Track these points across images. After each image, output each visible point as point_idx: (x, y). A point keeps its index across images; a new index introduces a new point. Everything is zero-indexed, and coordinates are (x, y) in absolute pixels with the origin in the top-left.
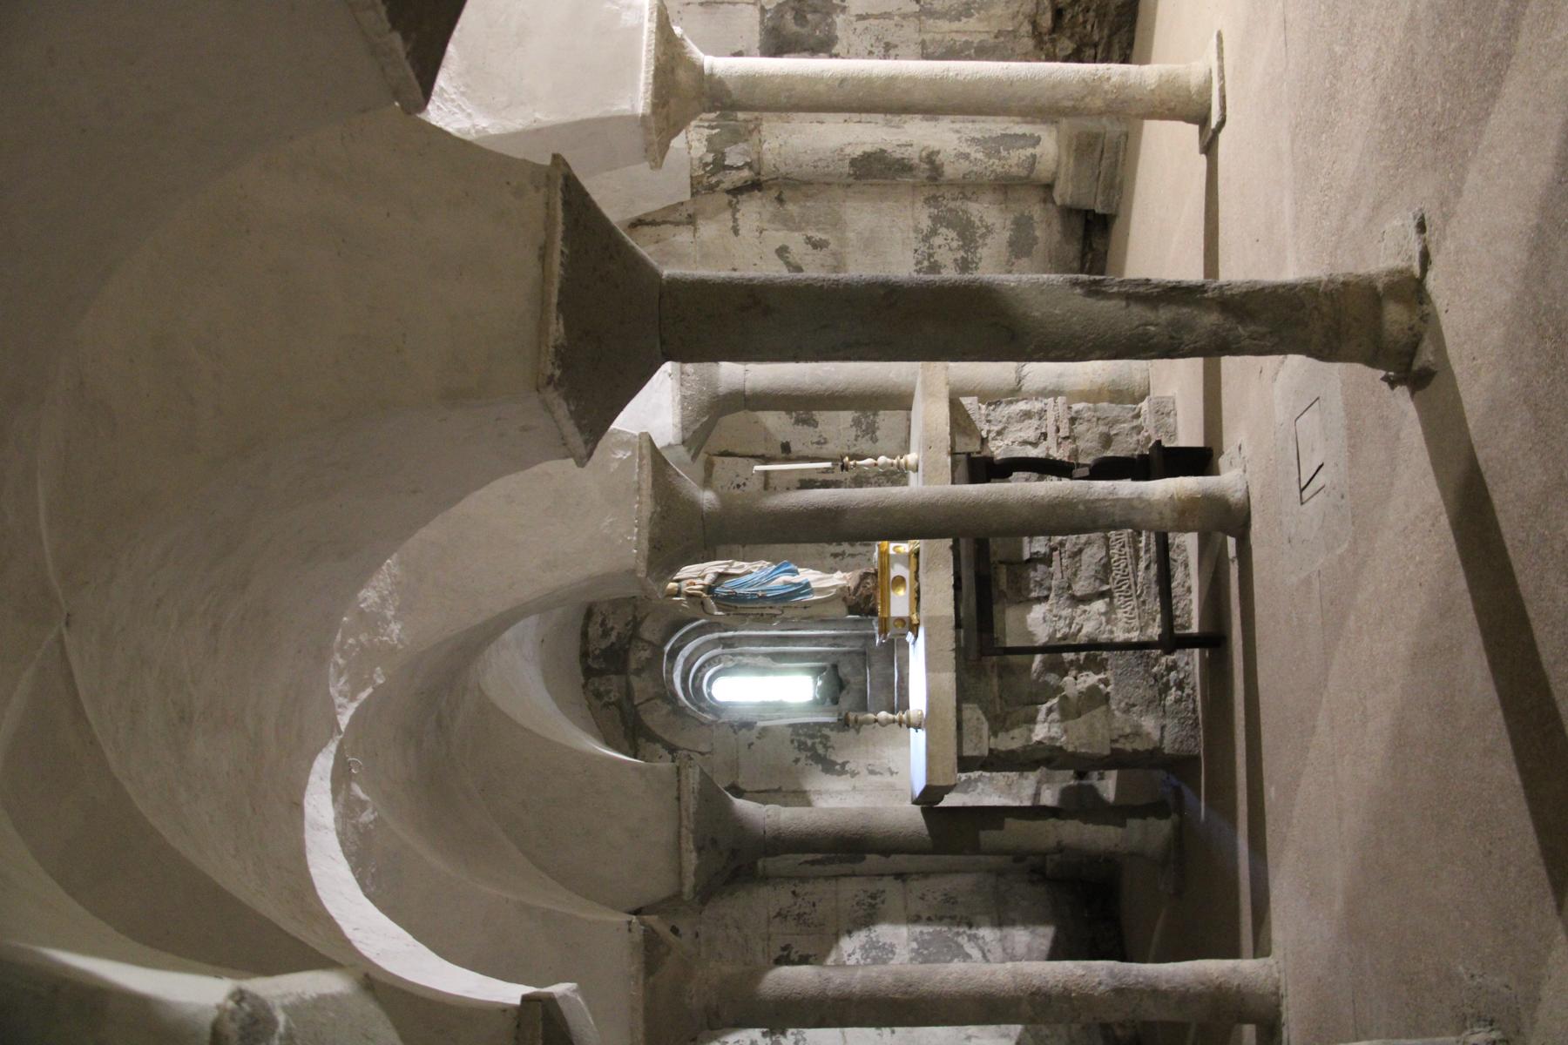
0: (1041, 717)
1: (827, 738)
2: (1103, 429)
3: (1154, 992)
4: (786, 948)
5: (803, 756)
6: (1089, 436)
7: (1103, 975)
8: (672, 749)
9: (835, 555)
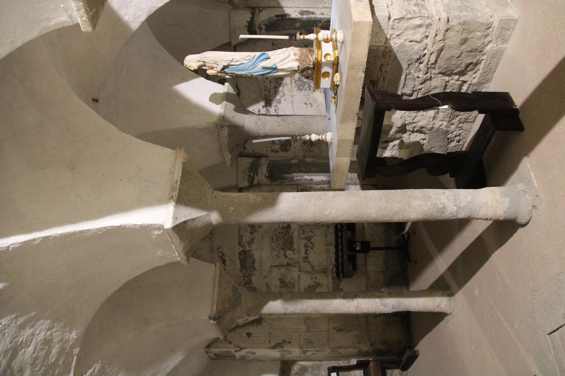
0: (389, 148)
2: (464, 36)
6: (454, 39)
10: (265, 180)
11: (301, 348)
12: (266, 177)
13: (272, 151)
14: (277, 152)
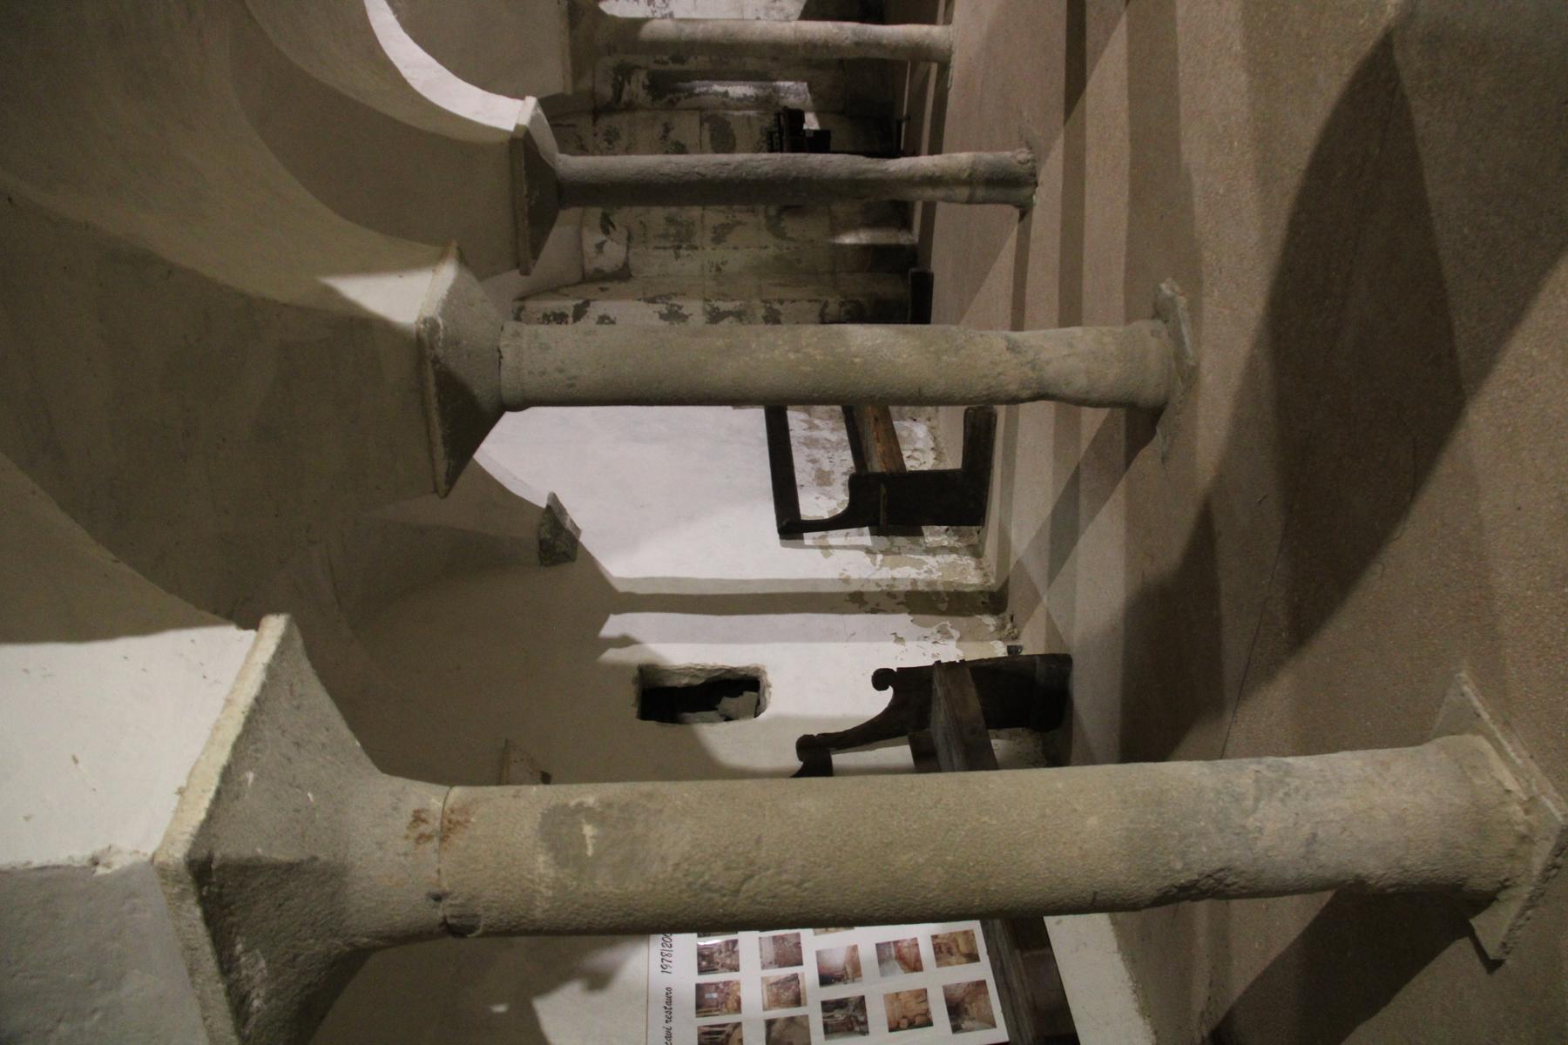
3: (878, 44)
7: (849, 33)
10: (643, 96)
11: (706, 300)
12: (644, 87)
13: (657, 62)
14: (665, 63)
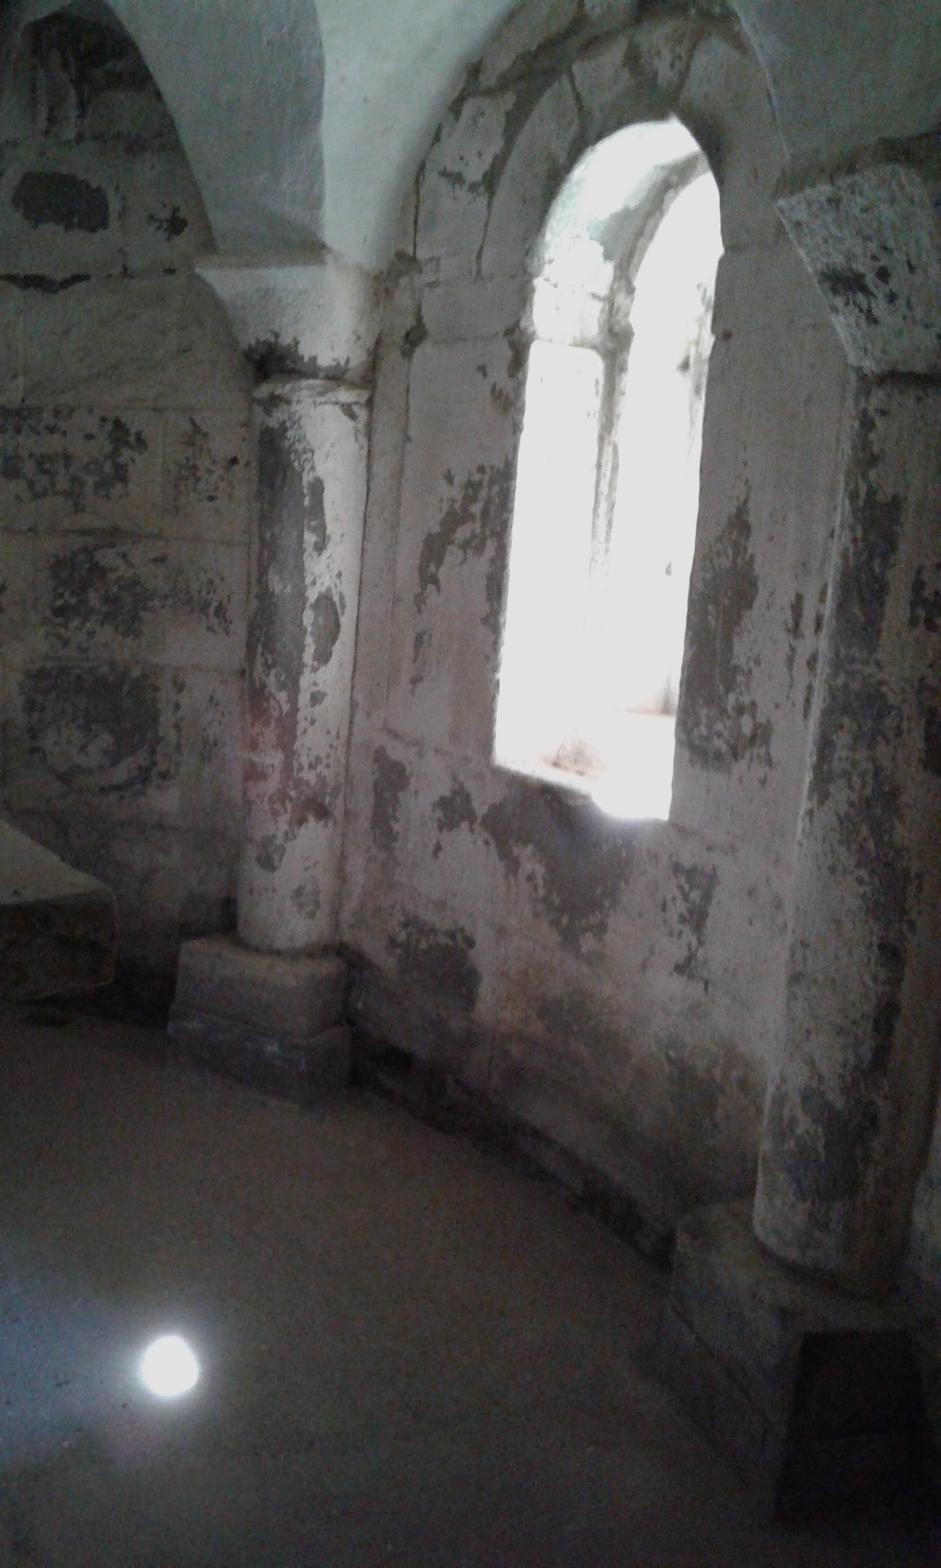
1: (480, 549)
4: (141, 442)
5: (456, 493)
8: (490, 181)
9: (797, 608)
